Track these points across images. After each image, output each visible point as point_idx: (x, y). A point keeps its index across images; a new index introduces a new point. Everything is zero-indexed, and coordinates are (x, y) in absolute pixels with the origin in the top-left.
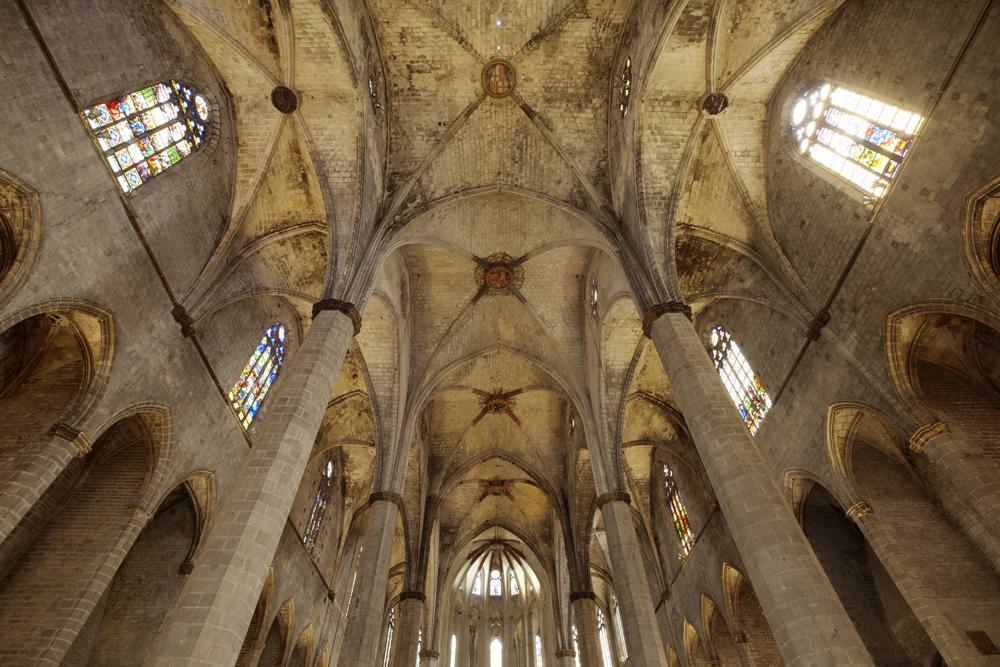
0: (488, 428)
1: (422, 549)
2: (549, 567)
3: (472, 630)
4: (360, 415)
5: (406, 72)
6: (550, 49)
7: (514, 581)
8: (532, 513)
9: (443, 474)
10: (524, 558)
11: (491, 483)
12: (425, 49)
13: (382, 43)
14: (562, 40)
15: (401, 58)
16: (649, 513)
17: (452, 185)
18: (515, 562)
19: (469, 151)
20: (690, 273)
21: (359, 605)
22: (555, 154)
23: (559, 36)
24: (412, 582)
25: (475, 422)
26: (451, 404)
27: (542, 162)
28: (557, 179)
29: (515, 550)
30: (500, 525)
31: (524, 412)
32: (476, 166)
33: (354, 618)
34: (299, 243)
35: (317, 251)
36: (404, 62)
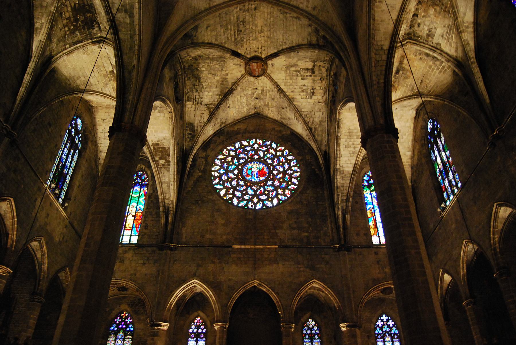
5: (316, 69)
6: (225, 83)
12: (301, 84)
13: (326, 89)
14: (218, 89)
15: (317, 78)
17: (294, 19)
19: (278, 33)
20: (74, 9)
22: (213, 41)
23: (221, 92)
27: (222, 31)
28: (209, 29)
32: (273, 21)
34: (428, 35)
35: (419, 21)
36: (316, 76)
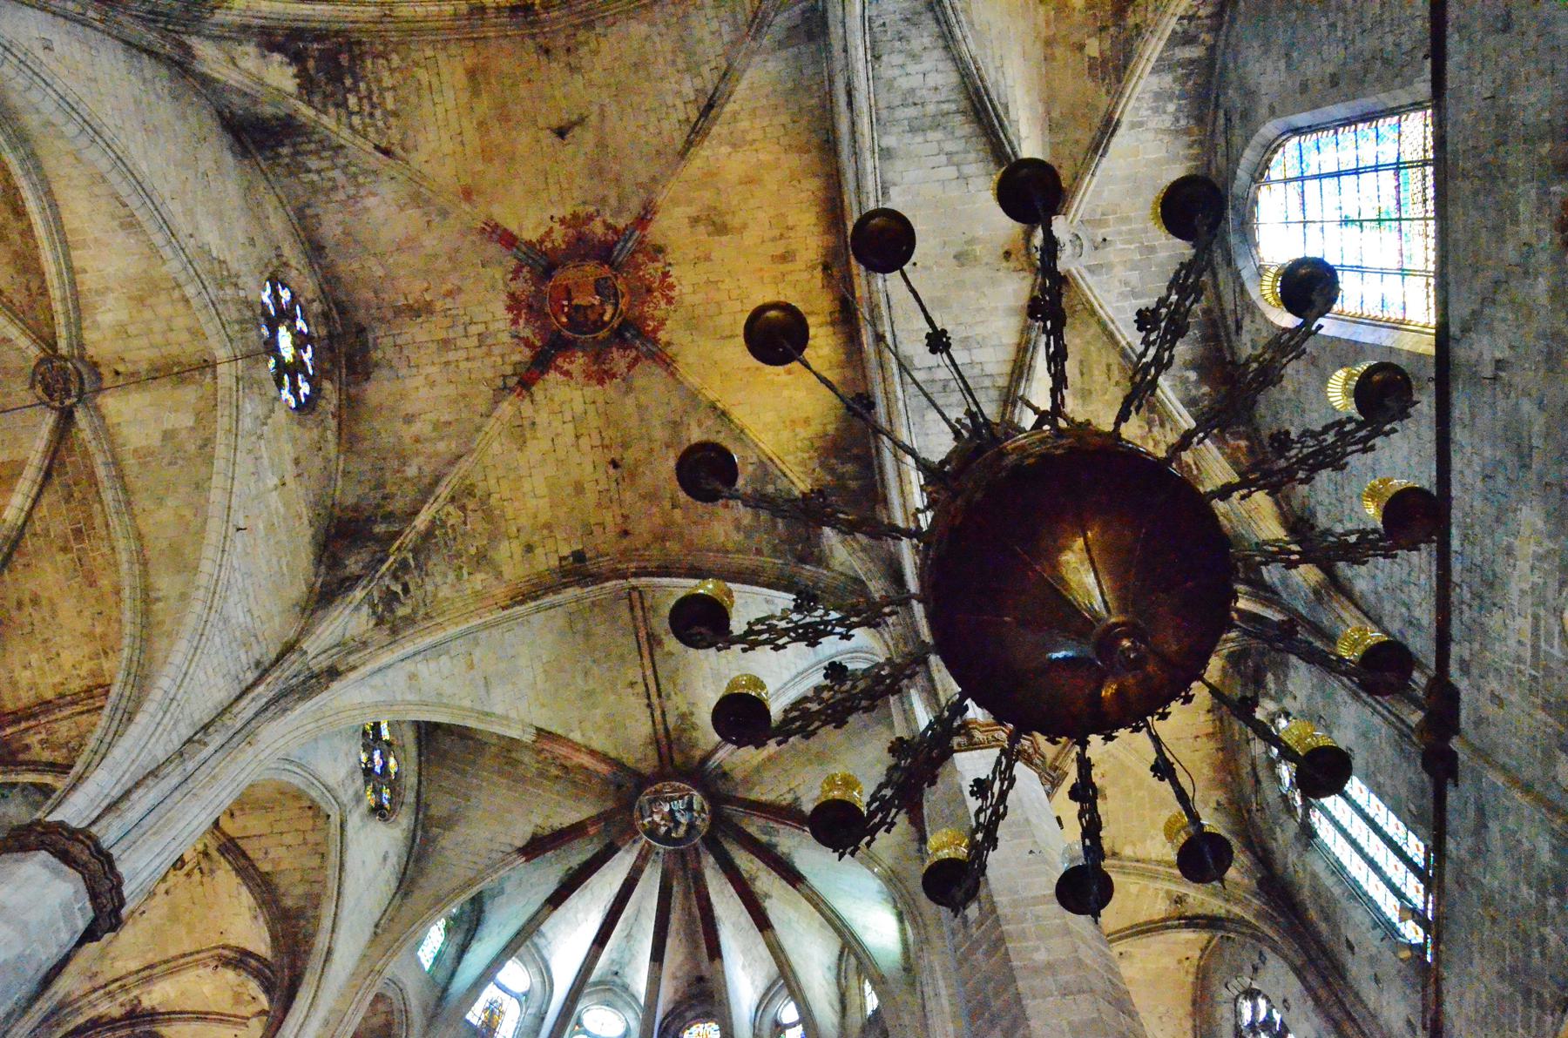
8: (769, 417)
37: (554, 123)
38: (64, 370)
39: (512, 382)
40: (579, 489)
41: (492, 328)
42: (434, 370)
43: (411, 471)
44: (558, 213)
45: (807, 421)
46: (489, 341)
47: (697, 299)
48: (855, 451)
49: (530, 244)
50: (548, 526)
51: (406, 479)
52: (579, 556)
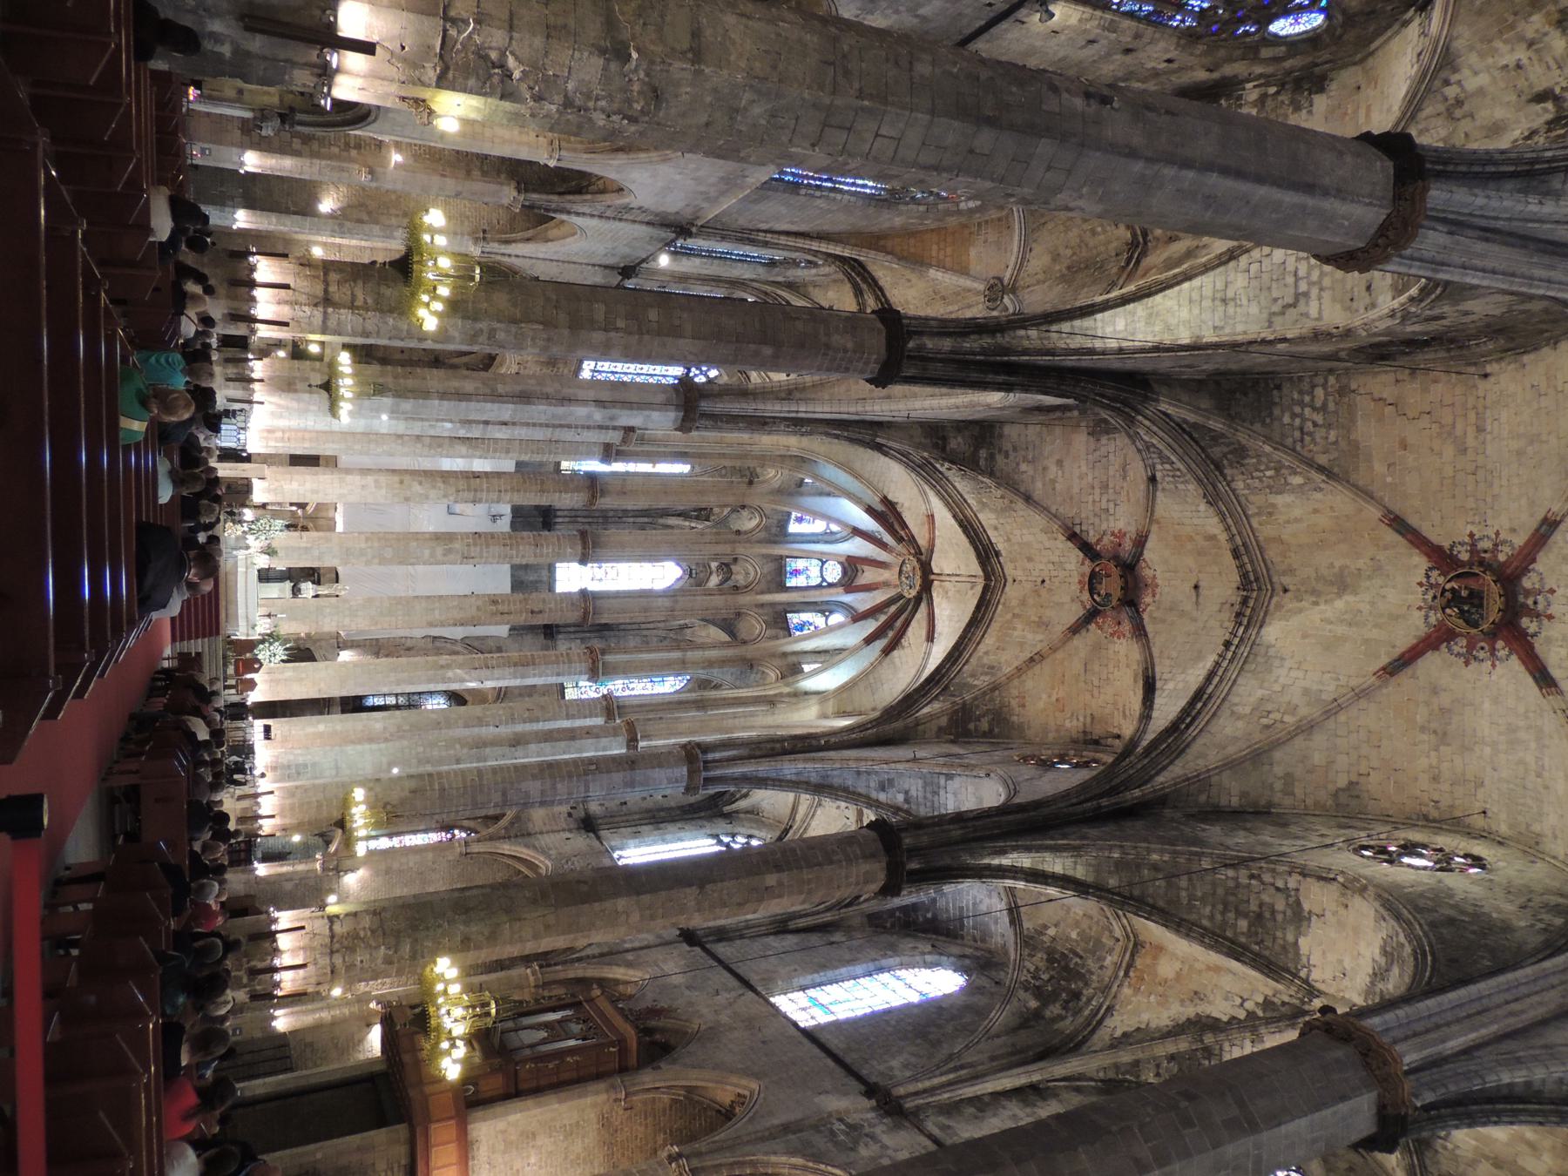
0: (1361, 563)
1: (1010, 368)
2: (889, 728)
3: (702, 514)
4: (1541, 97)
7: (819, 620)
8: (1029, 684)
9: (1216, 424)
10: (887, 651)
11: (1130, 568)
16: (1111, 1075)
18: (870, 626)
21: (1094, 106)
24: (930, 343)
25: (1398, 523)
26: (1471, 441)
29: (907, 624)
30: (986, 589)
31: (1435, 691)
33: (1054, 89)
37: (1201, 584)
38: (996, 300)
39: (1077, 530)
40: (1030, 559)
41: (1111, 518)
42: (1090, 478)
43: (1023, 467)
44: (1158, 574)
45: (1024, 706)
46: (1103, 516)
47: (1111, 652)
48: (996, 730)
49: (1141, 554)
50: (1009, 540)
51: (1018, 464)
52: (998, 554)
